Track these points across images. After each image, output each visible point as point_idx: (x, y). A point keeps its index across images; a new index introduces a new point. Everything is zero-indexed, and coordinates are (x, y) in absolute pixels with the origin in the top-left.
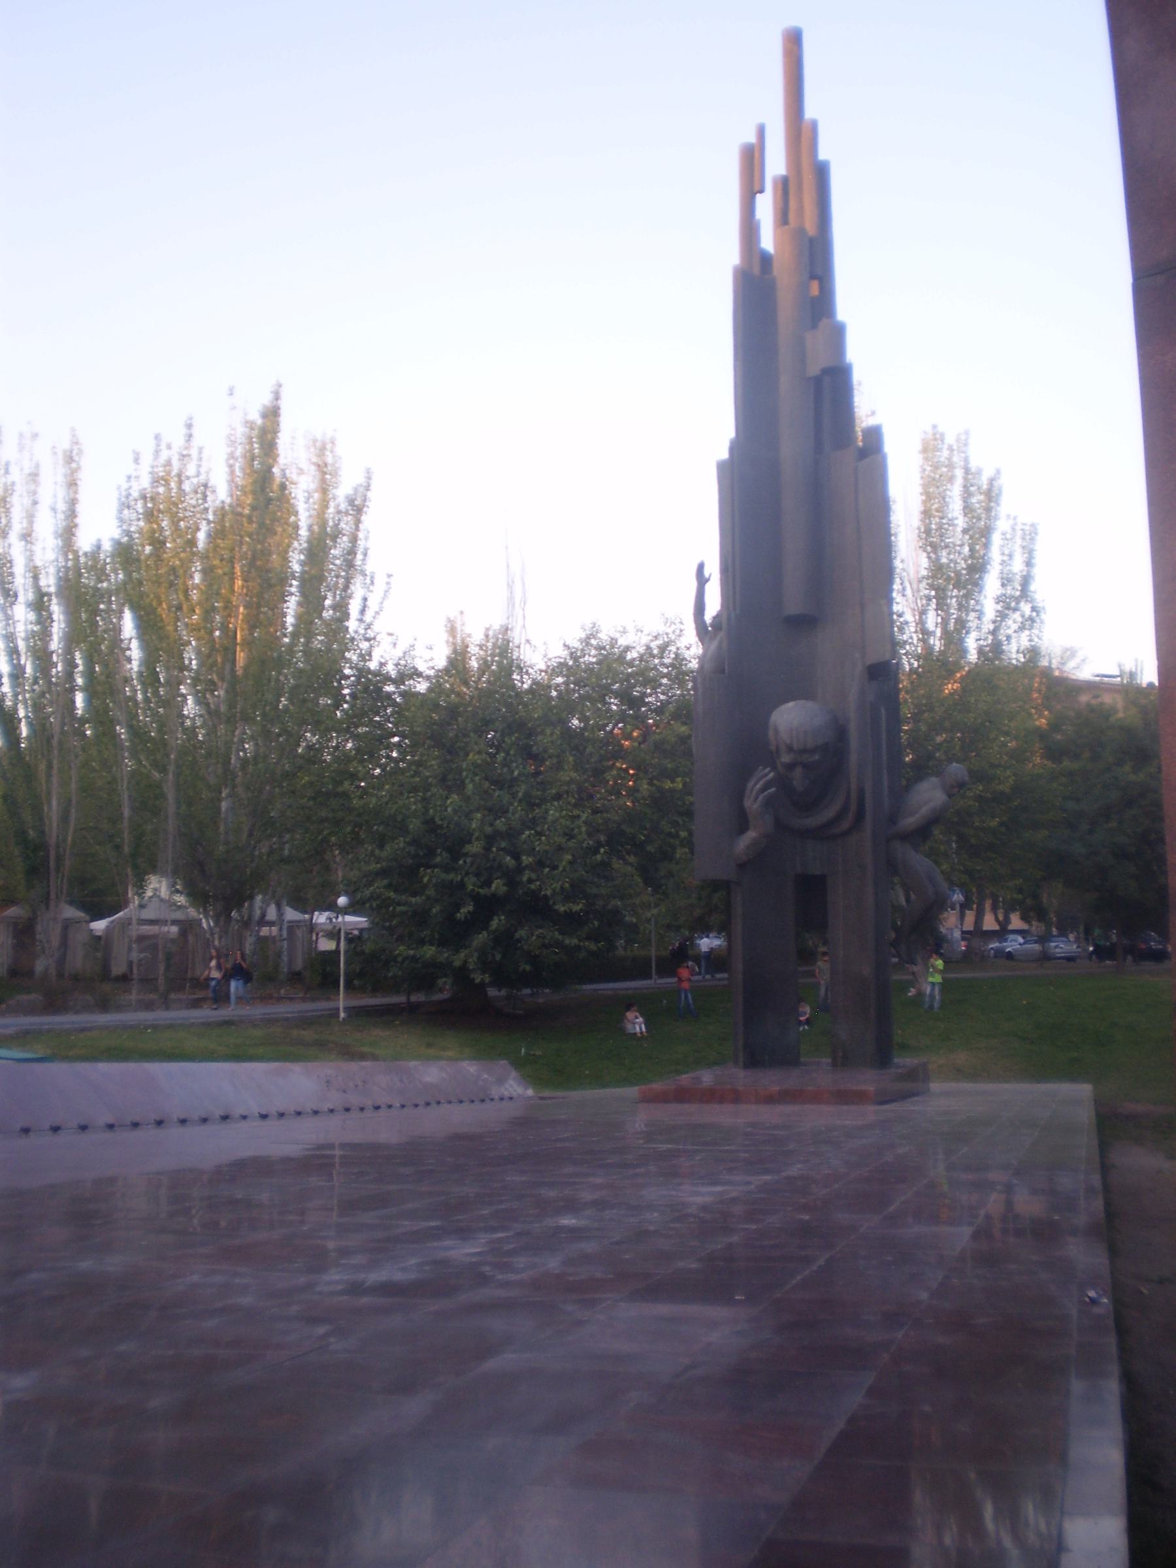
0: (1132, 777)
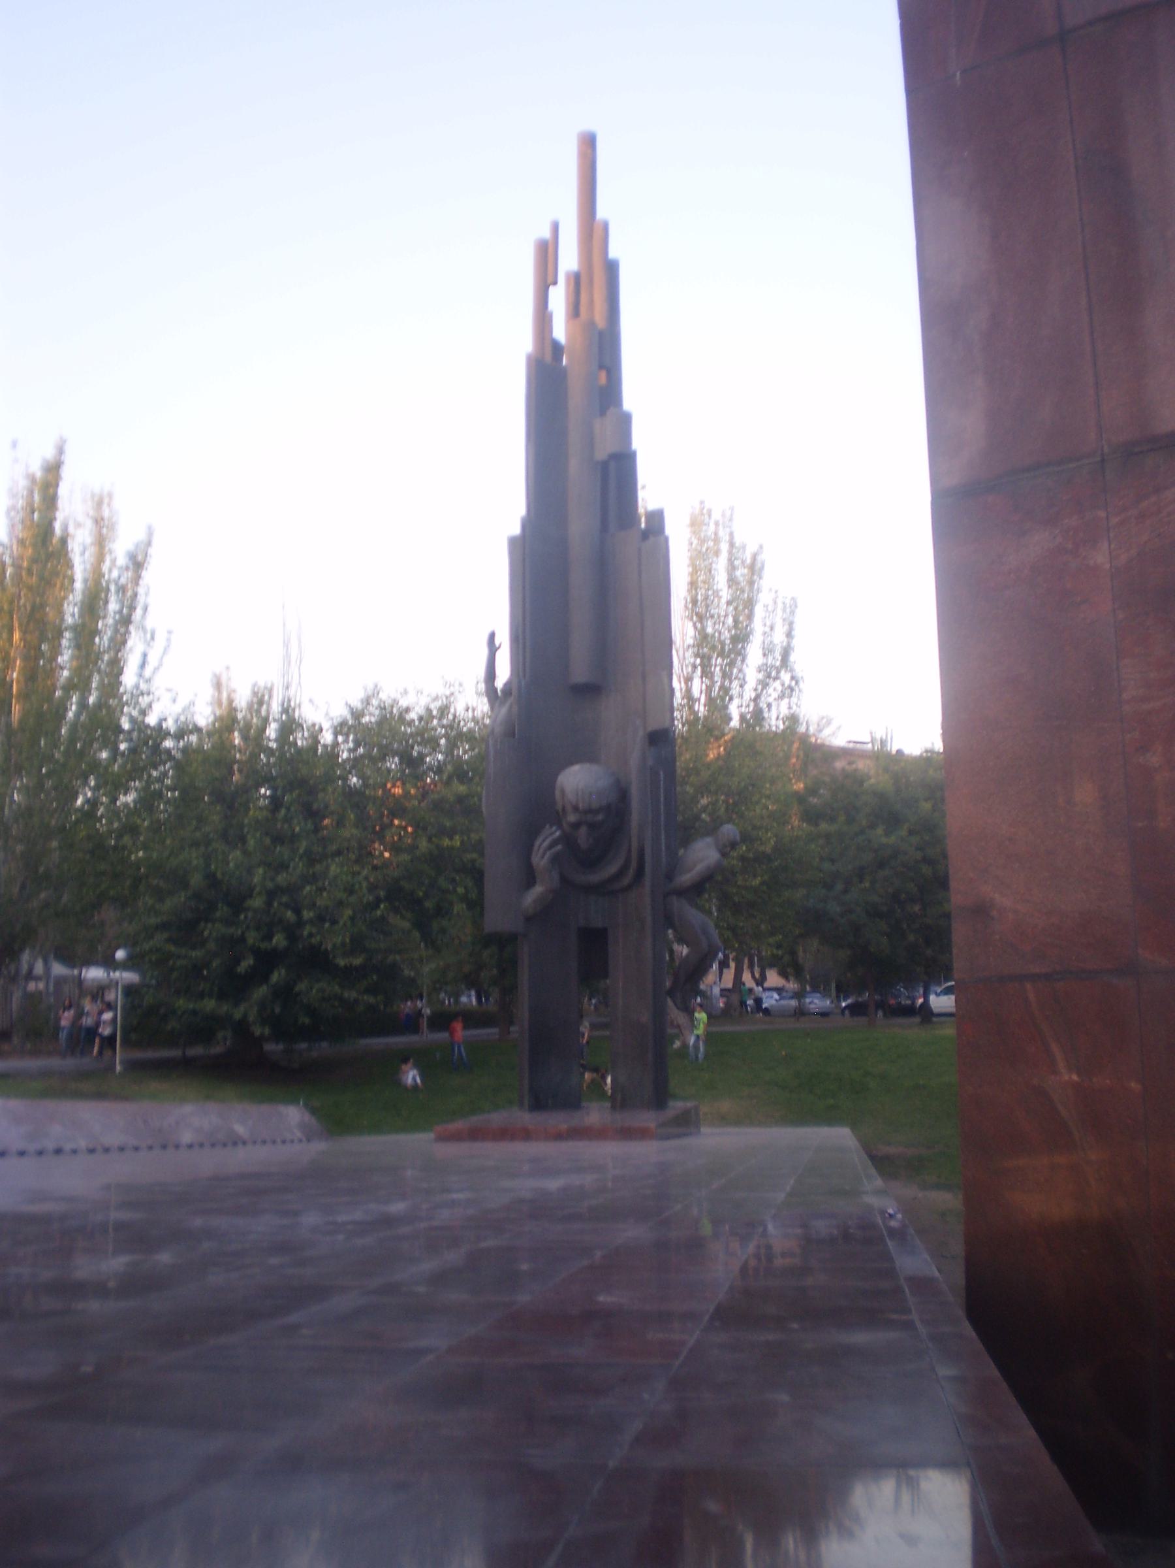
0: (884, 840)
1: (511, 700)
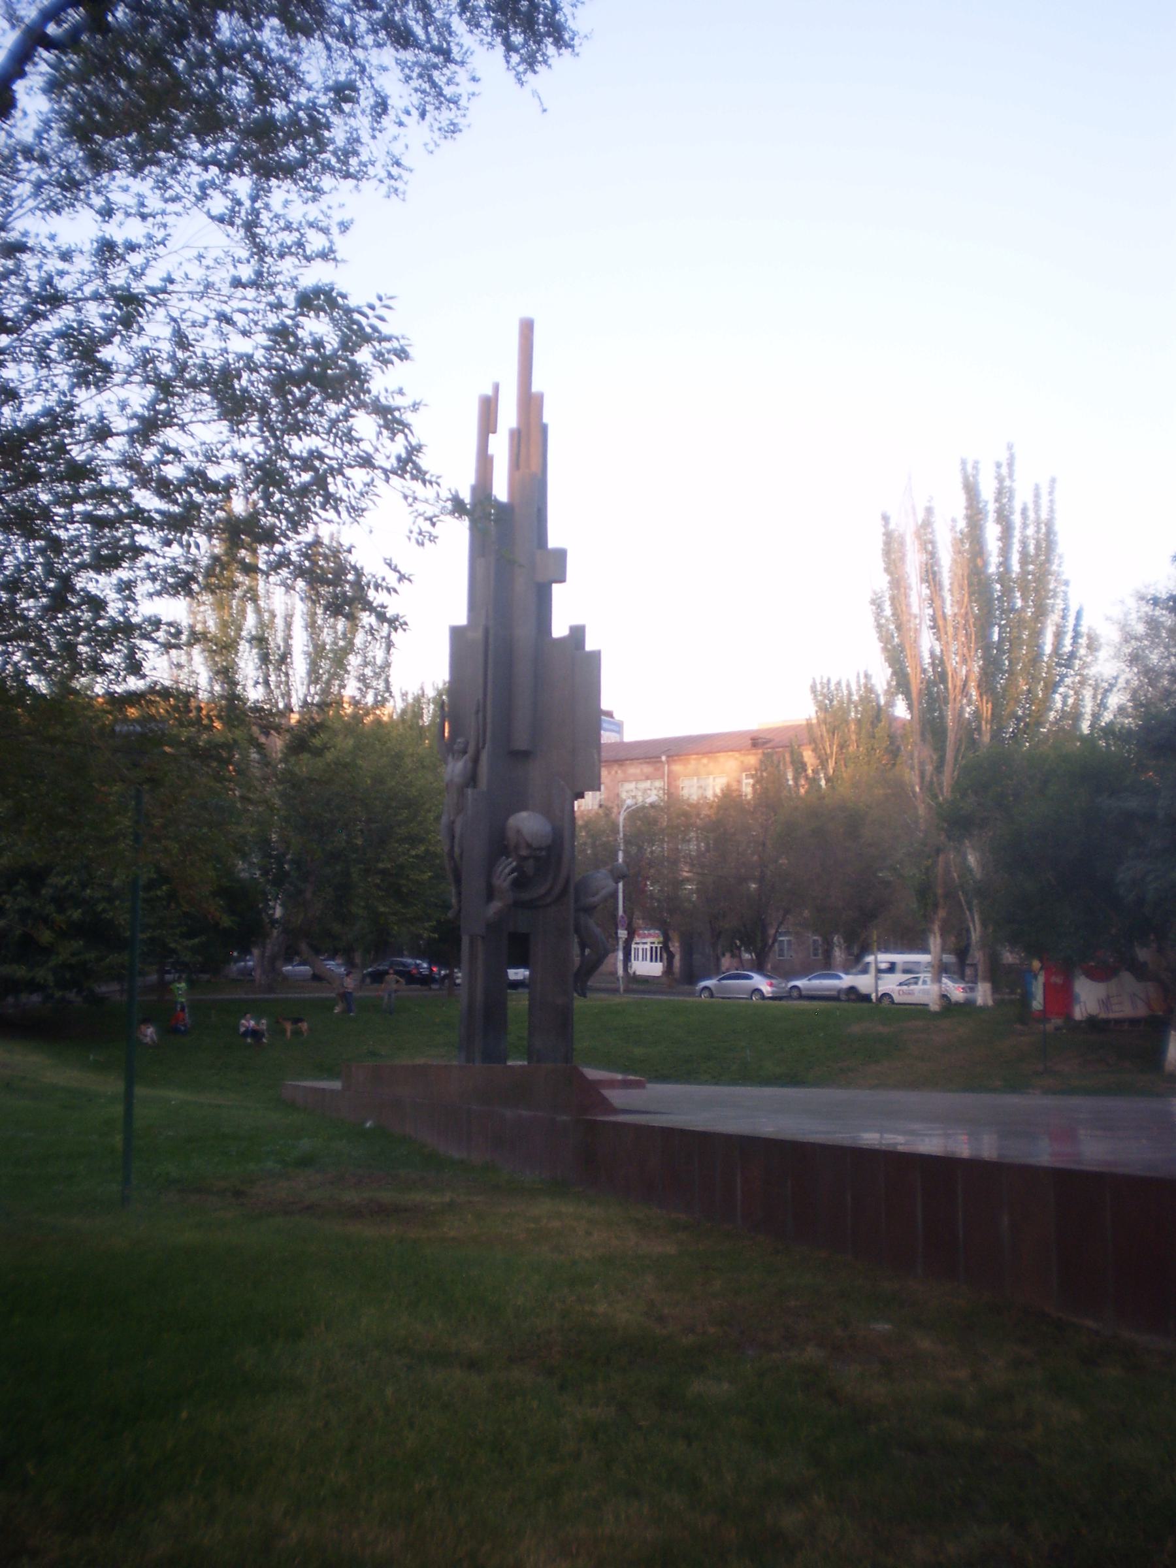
1: (467, 756)
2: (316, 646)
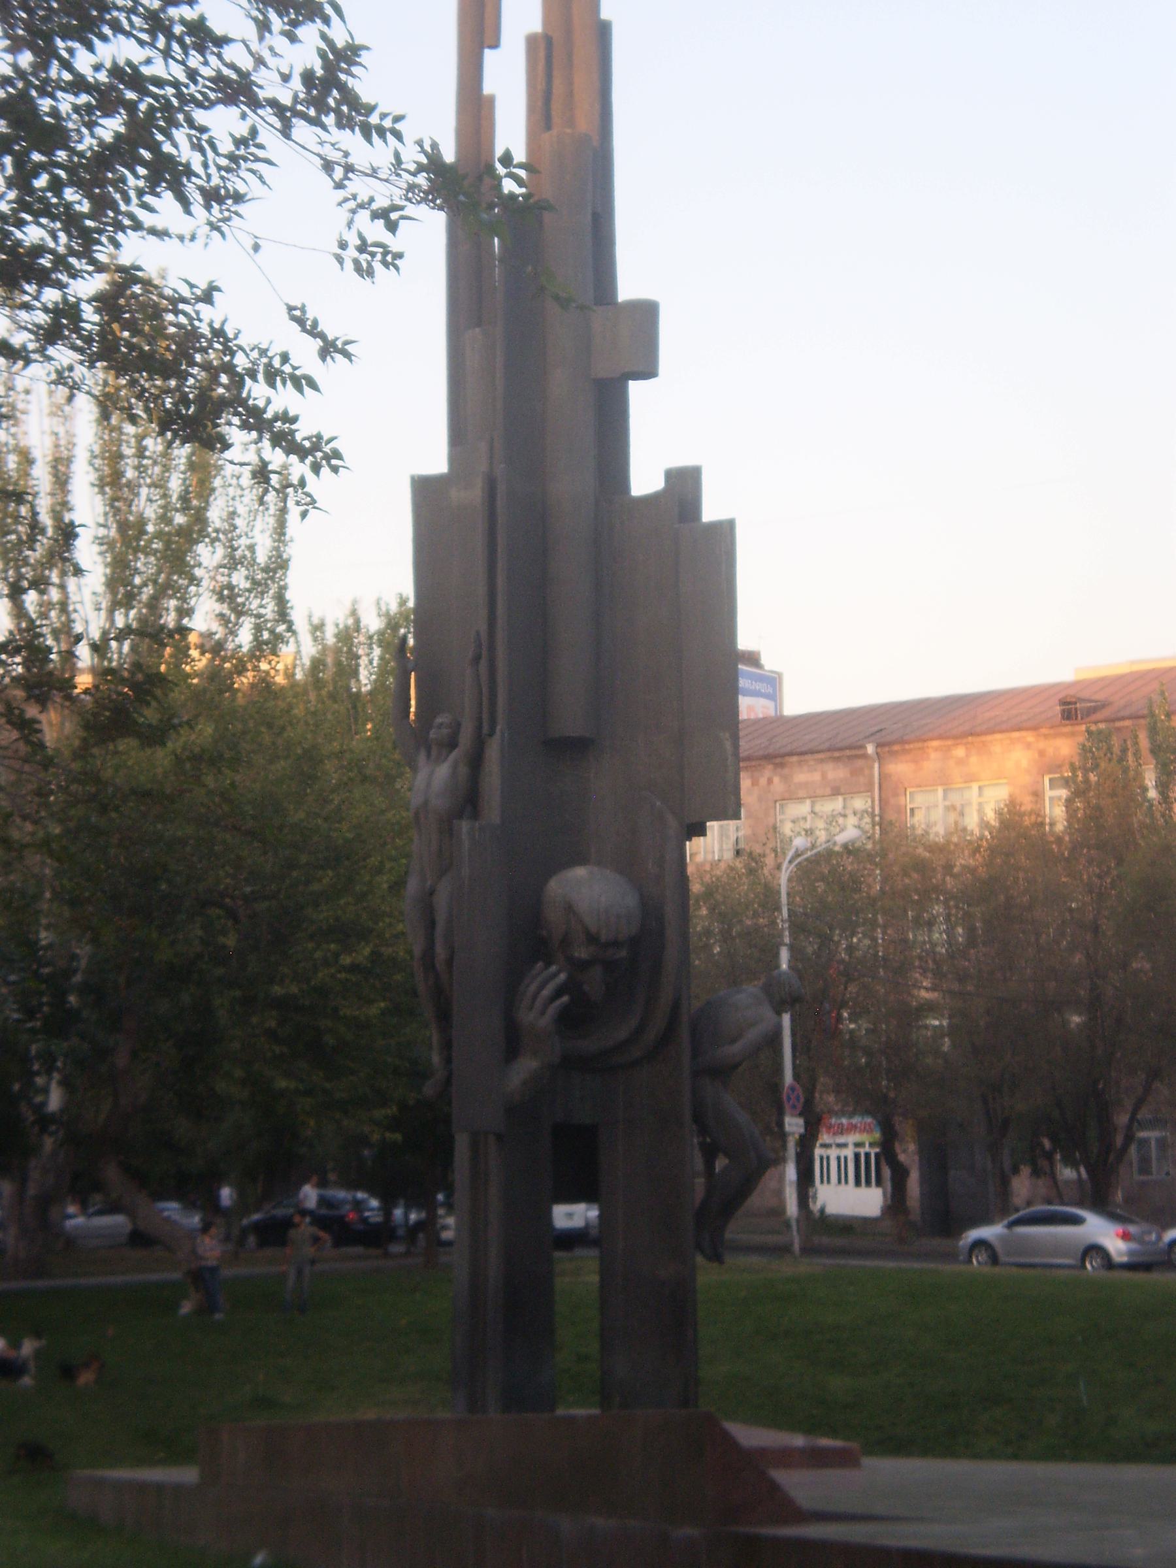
2: (123, 526)
